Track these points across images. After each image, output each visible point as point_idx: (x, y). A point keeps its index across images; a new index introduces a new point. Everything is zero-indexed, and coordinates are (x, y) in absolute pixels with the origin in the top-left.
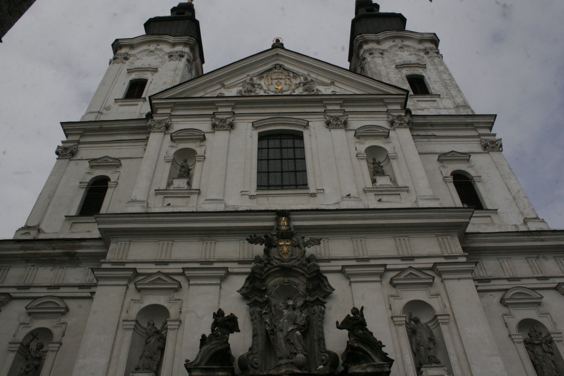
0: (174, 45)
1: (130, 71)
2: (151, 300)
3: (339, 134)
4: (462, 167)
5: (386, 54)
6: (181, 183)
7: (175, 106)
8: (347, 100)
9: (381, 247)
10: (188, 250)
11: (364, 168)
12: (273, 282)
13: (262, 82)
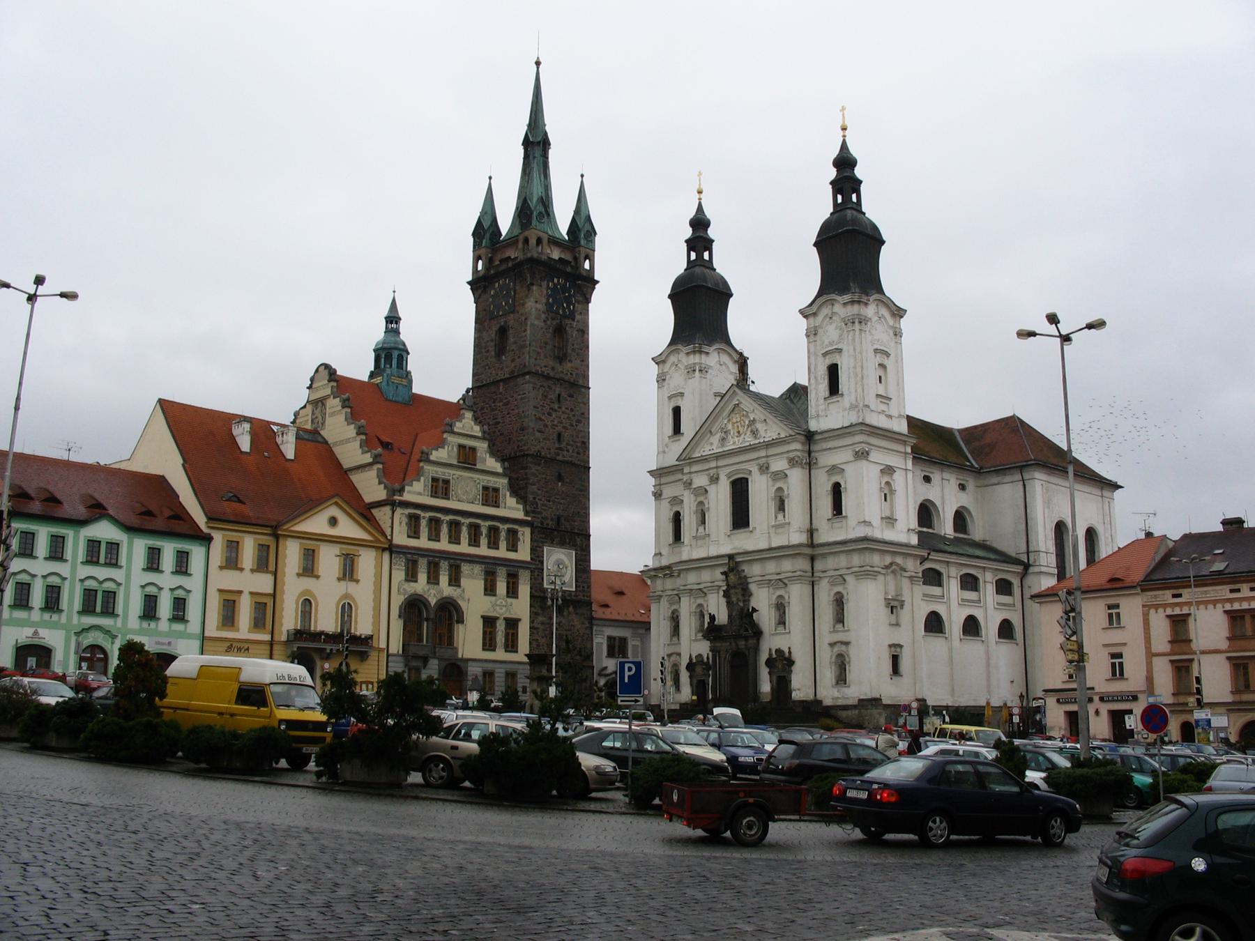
0: (688, 354)
1: (670, 398)
2: (700, 601)
3: (764, 477)
4: (837, 478)
5: (820, 331)
6: (701, 529)
7: (690, 464)
8: (768, 445)
9: (771, 567)
10: (706, 576)
11: (773, 507)
12: (732, 591)
13: (730, 426)
